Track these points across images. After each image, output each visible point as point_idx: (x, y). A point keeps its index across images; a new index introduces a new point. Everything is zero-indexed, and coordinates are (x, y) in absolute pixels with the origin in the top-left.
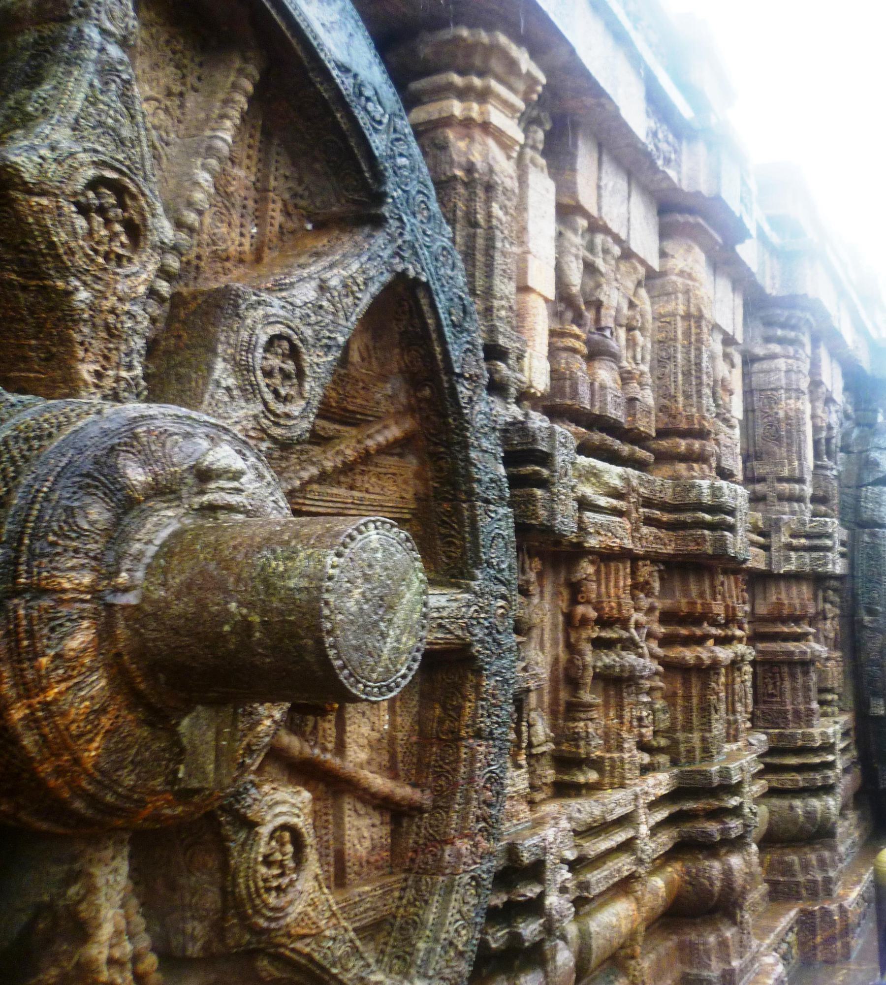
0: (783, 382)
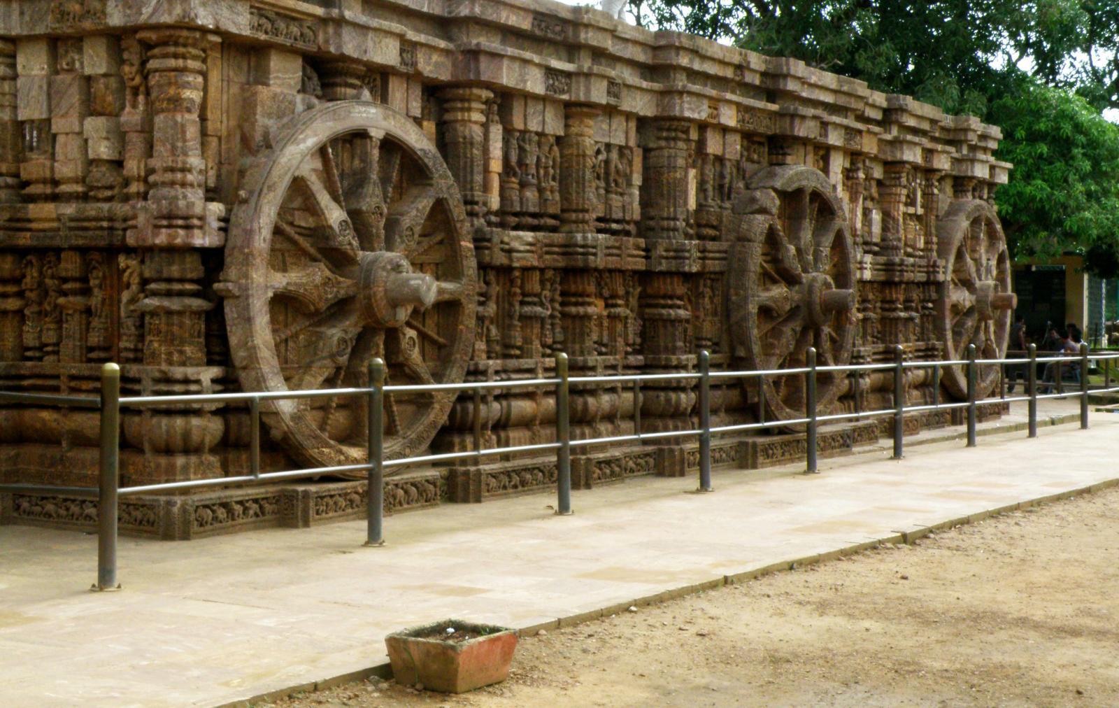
0: (666, 163)
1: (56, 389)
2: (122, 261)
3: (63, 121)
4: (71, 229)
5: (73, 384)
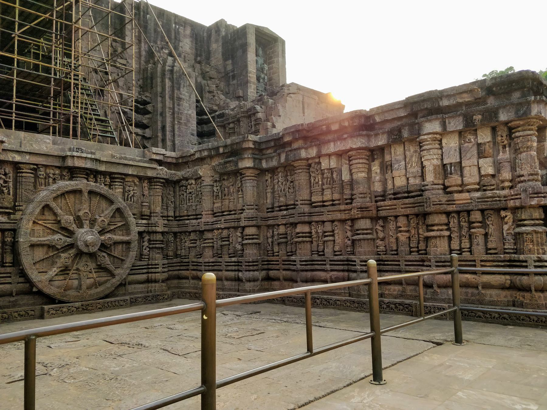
1: (475, 266)
2: (503, 213)
3: (468, 161)
4: (478, 202)
5: (483, 263)
